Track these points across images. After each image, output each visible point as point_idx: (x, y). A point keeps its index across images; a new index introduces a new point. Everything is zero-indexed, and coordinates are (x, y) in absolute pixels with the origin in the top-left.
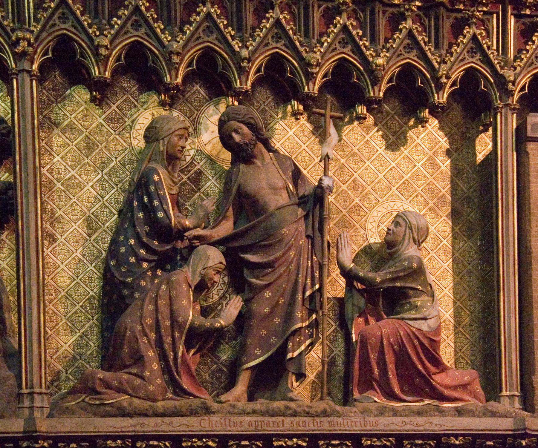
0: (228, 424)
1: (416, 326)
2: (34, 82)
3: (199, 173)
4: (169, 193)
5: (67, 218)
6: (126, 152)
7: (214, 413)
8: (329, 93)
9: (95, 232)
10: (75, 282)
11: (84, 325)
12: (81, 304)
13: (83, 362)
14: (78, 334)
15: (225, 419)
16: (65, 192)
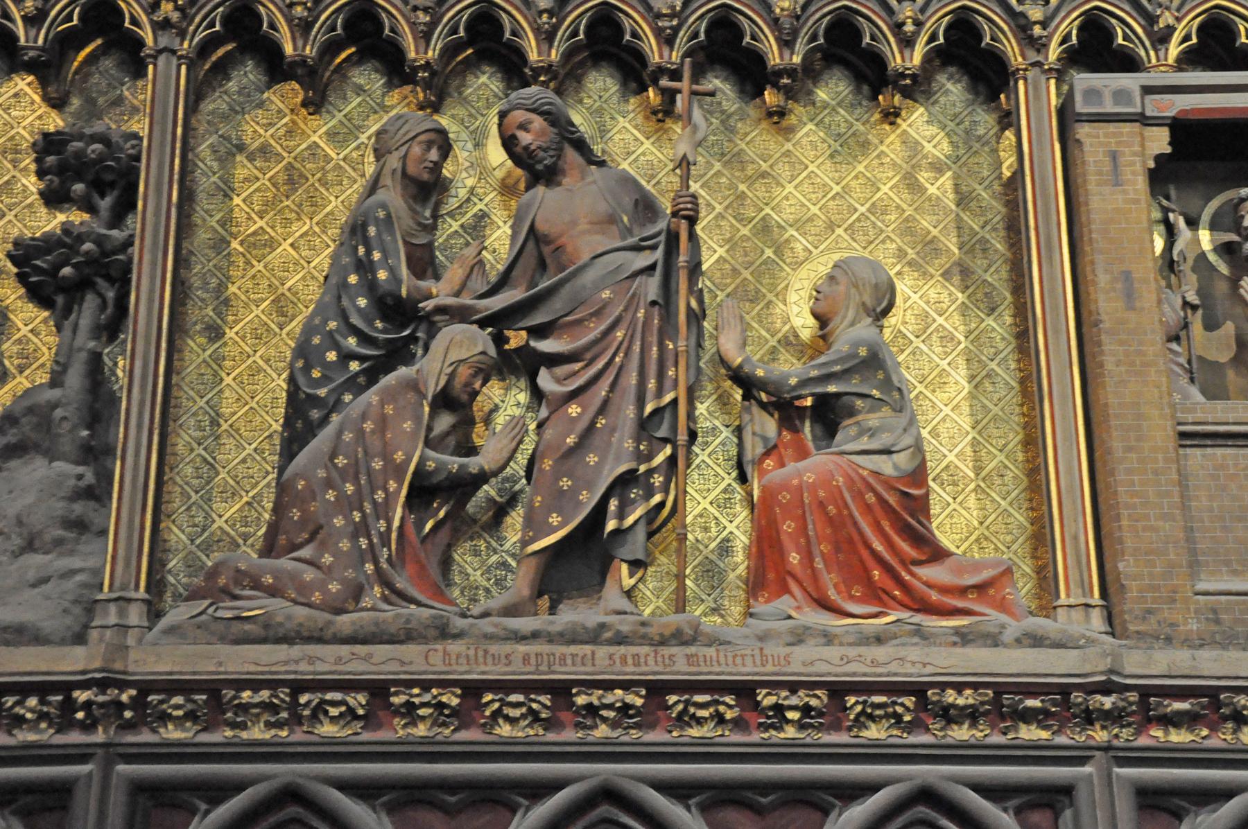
0: (481, 660)
1: (871, 466)
2: (184, 68)
3: (482, 216)
4: (406, 243)
5: (243, 297)
6: (355, 186)
7: (456, 636)
8: (716, 77)
9: (291, 320)
10: (247, 408)
11: (257, 483)
12: (254, 446)
13: (249, 550)
14: (245, 499)
15: (476, 649)
16: (244, 256)
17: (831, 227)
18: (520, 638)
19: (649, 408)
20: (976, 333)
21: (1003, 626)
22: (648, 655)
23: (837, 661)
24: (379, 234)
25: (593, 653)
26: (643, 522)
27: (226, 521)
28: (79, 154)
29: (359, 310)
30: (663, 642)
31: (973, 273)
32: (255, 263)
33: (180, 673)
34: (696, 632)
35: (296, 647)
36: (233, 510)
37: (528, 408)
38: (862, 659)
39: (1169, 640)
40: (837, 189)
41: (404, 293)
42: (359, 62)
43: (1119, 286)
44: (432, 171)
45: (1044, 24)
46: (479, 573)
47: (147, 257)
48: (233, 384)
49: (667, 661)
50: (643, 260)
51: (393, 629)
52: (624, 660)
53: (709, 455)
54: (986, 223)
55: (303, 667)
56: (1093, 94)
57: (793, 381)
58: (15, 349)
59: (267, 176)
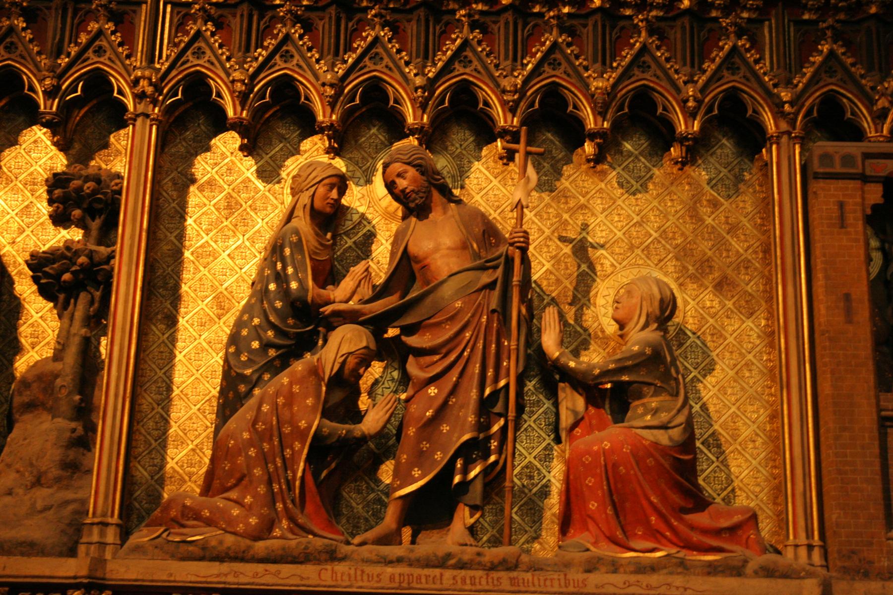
0: (359, 578)
4: (311, 259)
5: (192, 295)
6: (277, 211)
8: (549, 132)
9: (227, 312)
10: (193, 378)
11: (200, 435)
12: (198, 406)
13: (193, 485)
14: (191, 447)
15: (356, 570)
16: (194, 263)
17: (632, 248)
18: (389, 562)
19: (488, 391)
20: (738, 331)
21: (746, 562)
22: (481, 577)
23: (622, 586)
24: (292, 253)
25: (441, 575)
26: (480, 477)
27: (177, 463)
28: (80, 189)
29: (275, 310)
30: (493, 567)
31: (738, 285)
32: (202, 268)
33: (143, 580)
34: (517, 560)
35: (225, 564)
36: (181, 455)
37: (400, 382)
38: (640, 584)
39: (866, 575)
40: (636, 219)
41: (309, 299)
42: (282, 118)
43: (842, 304)
44: (332, 206)
45: (792, 103)
46: (360, 507)
47: (124, 270)
48: (184, 361)
49: (495, 582)
50: (486, 278)
51: (295, 553)
52: (464, 580)
53: (535, 421)
54: (749, 247)
55: (230, 579)
56: (826, 158)
57: (597, 372)
58: (30, 330)
59: (212, 203)
